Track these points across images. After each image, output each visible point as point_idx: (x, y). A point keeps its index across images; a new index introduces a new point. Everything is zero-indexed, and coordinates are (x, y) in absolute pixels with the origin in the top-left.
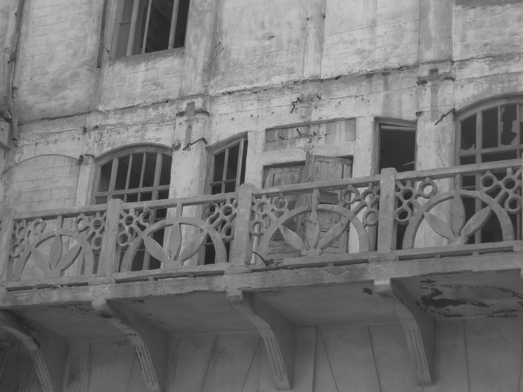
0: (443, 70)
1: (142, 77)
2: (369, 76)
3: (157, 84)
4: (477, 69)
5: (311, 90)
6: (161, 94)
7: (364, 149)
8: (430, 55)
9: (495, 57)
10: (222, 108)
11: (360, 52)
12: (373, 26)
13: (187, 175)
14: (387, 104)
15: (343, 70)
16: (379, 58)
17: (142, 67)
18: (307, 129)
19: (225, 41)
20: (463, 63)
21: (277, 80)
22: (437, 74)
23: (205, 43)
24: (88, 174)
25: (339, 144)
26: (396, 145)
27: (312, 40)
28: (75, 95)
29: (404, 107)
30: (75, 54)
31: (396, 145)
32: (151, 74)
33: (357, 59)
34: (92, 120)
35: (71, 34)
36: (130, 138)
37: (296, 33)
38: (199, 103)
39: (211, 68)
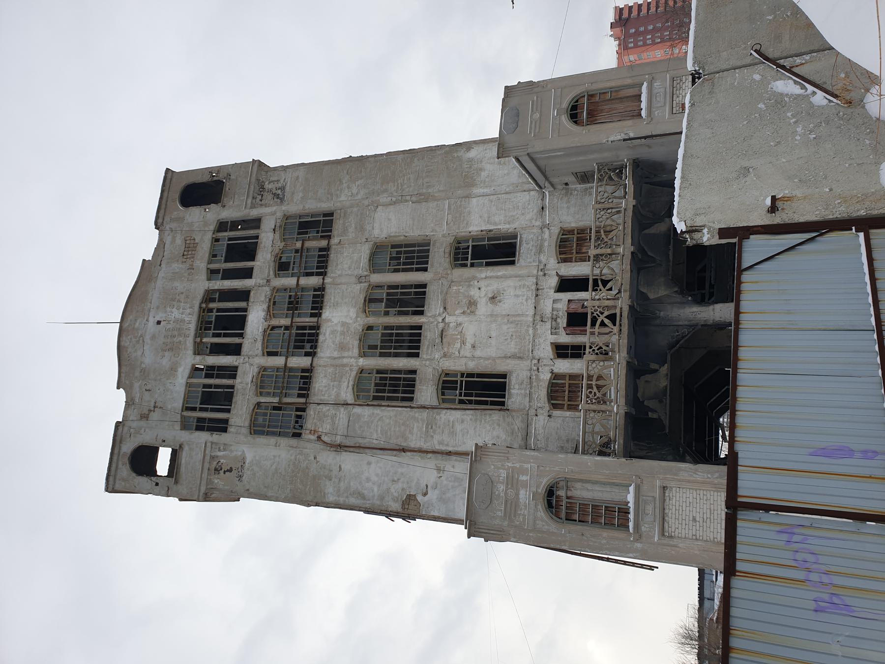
0: (542, 267)
1: (516, 395)
2: (537, 295)
3: (522, 383)
4: (543, 258)
5: (538, 318)
6: (526, 381)
7: (566, 296)
8: (535, 272)
9: (540, 250)
10: (538, 353)
11: (527, 300)
12: (517, 296)
13: (565, 366)
14: (550, 288)
15: (532, 306)
16: (531, 294)
17: (513, 391)
18: (554, 319)
19: (509, 355)
20: (540, 262)
21: (531, 331)
22: (543, 270)
23: (508, 361)
24: (557, 413)
25: (562, 307)
26: (566, 285)
27: (518, 319)
28: (518, 423)
29: (554, 281)
30: (499, 425)
31: (566, 285)
32: (517, 387)
33: (529, 301)
34: (532, 412)
35: (488, 428)
36: (543, 393)
37: (513, 325)
38: (535, 361)
39: (520, 358)
